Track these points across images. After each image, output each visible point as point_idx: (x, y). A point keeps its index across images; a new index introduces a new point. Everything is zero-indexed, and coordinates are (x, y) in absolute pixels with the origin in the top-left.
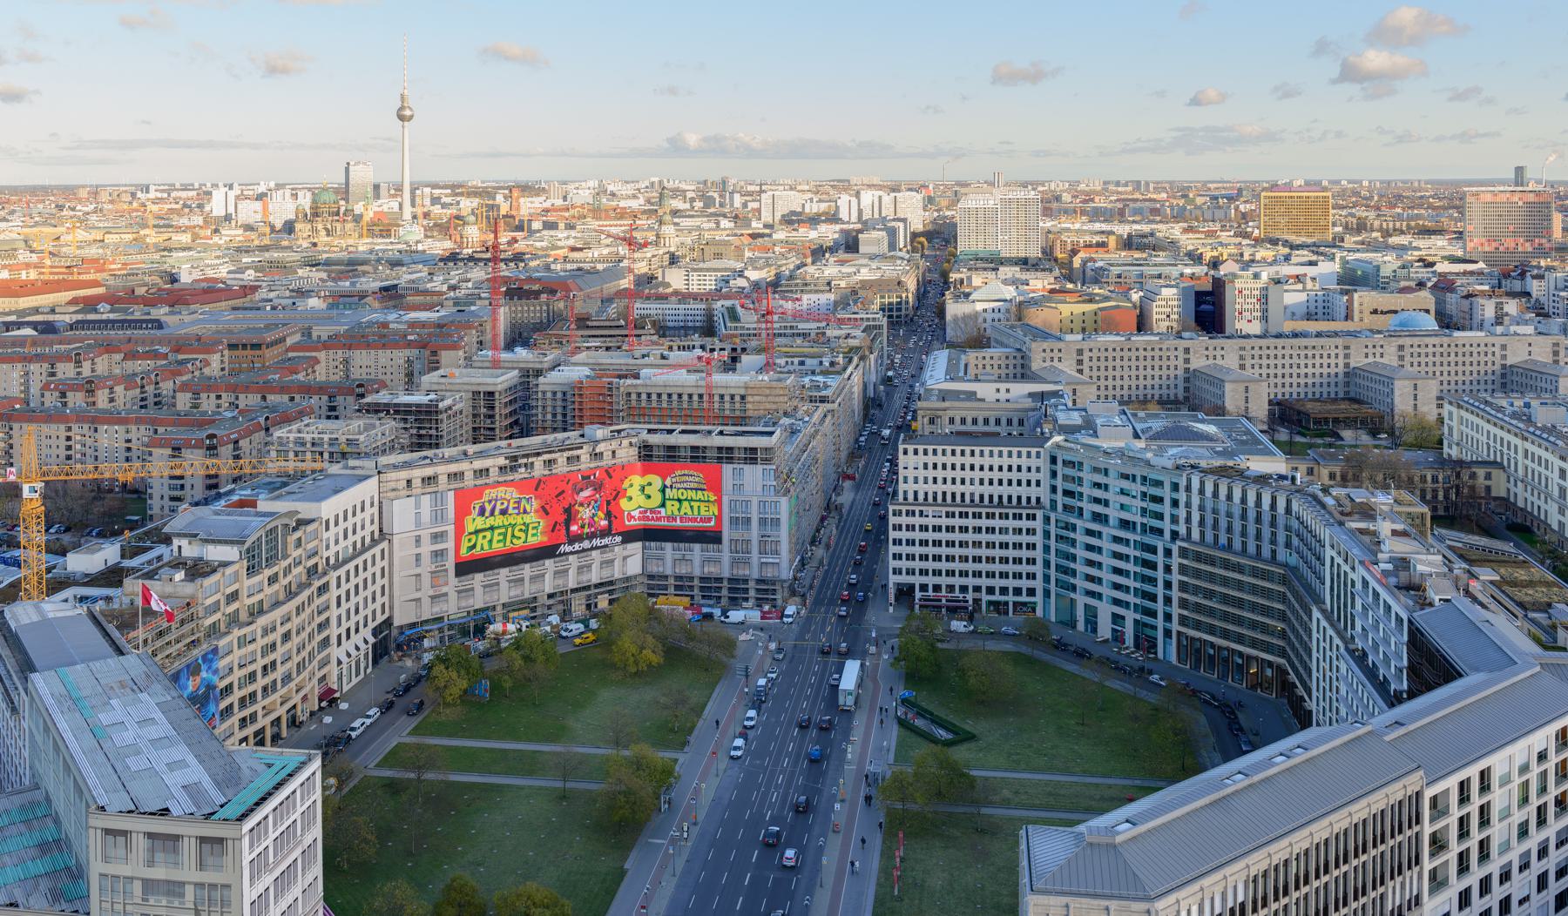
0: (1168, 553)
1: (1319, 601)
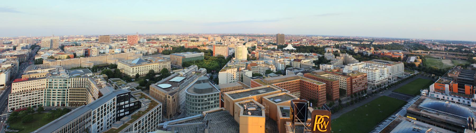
0: (68, 90)
1: (90, 91)
